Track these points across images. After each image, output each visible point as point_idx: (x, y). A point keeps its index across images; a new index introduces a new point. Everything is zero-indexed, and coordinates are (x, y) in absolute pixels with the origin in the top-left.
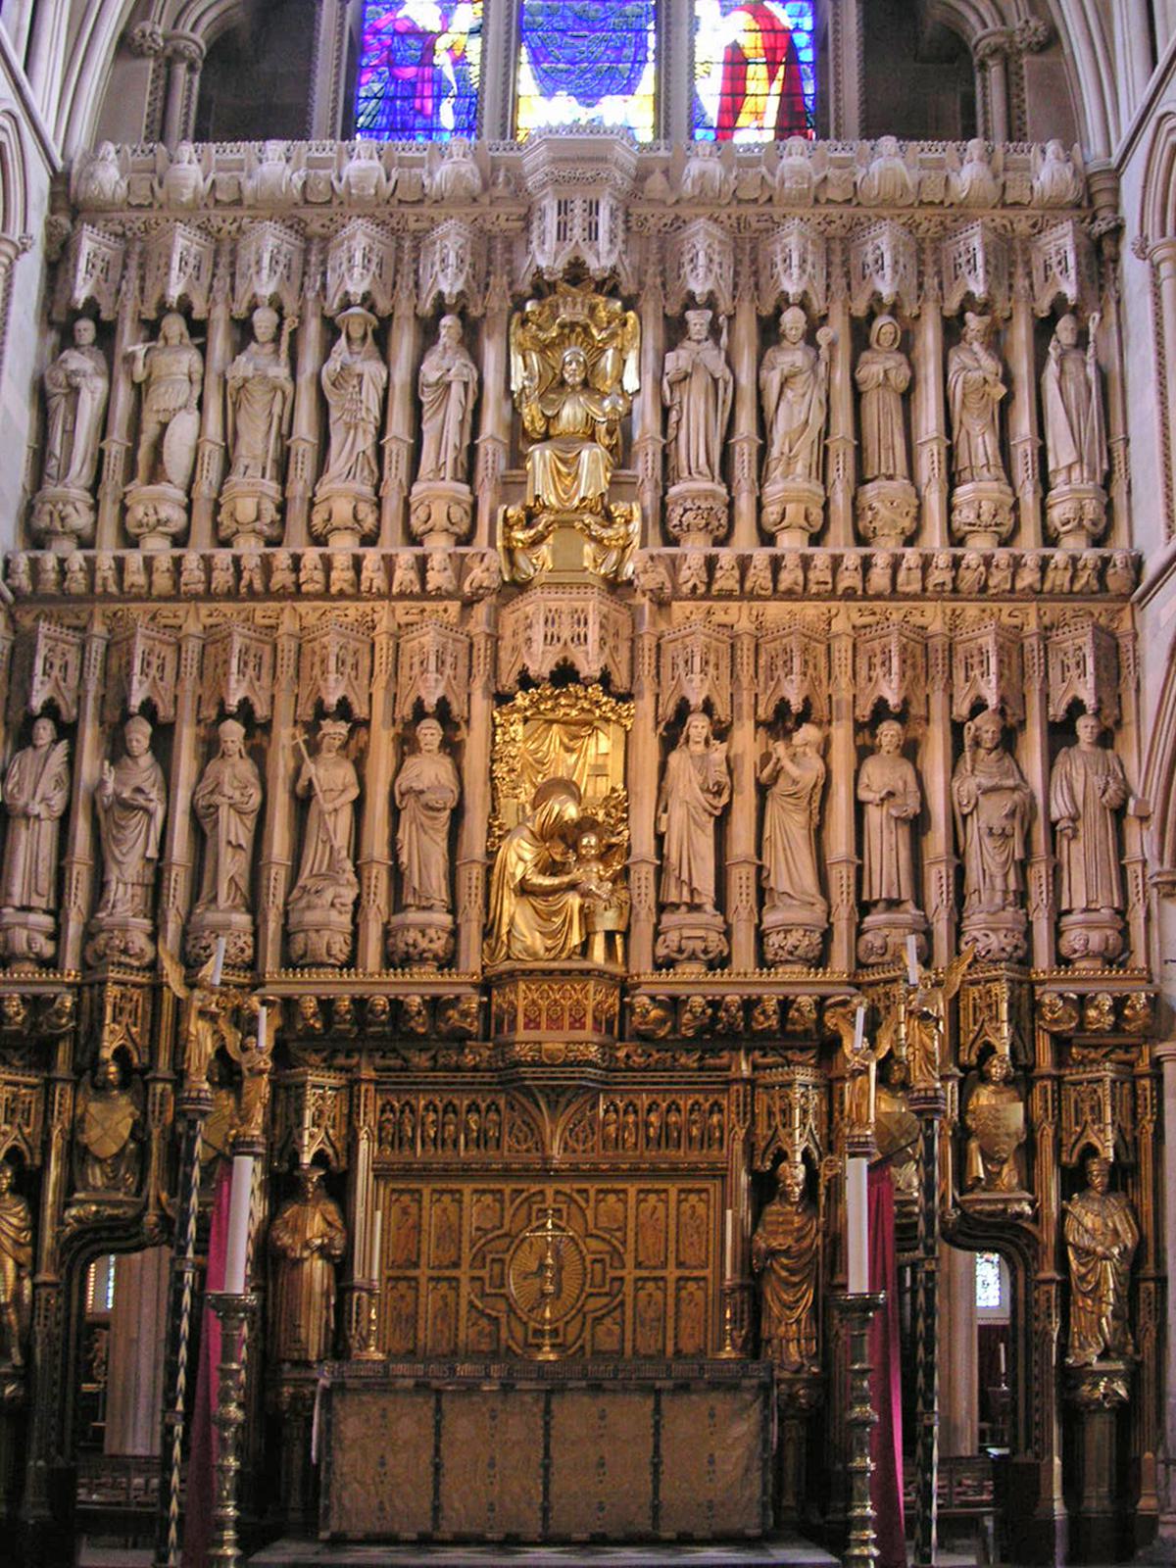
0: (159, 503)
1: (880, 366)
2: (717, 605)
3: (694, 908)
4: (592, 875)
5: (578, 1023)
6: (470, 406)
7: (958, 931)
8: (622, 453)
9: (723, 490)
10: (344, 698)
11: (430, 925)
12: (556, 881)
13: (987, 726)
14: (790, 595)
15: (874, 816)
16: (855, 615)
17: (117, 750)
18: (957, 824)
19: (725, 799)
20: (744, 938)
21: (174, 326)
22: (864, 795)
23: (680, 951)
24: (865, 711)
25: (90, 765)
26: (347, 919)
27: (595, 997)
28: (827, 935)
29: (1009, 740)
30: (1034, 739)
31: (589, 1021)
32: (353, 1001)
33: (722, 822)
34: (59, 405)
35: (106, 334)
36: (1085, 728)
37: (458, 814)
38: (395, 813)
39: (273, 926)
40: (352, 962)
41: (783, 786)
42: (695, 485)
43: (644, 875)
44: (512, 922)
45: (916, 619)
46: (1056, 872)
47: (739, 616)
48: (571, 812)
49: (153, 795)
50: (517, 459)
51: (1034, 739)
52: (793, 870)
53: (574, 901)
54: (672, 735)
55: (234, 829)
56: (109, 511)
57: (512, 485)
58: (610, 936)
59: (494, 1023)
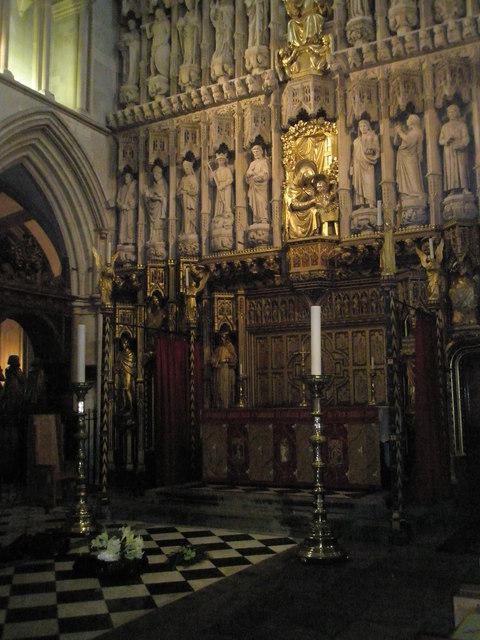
0: (155, 82)
2: (370, 71)
3: (367, 206)
5: (315, 262)
6: (266, 12)
9: (369, 18)
10: (224, 144)
11: (258, 229)
12: (306, 204)
14: (398, 58)
15: (447, 151)
16: (431, 59)
17: (152, 182)
19: (376, 157)
22: (442, 142)
23: (359, 226)
24: (440, 104)
25: (143, 187)
26: (230, 231)
28: (427, 209)
31: (319, 260)
32: (228, 264)
33: (377, 166)
34: (124, 54)
37: (270, 181)
38: (247, 187)
39: (204, 238)
40: (234, 248)
41: (403, 145)
43: (344, 196)
44: (289, 224)
45: (463, 54)
47: (377, 73)
48: (311, 173)
49: (160, 194)
53: (314, 211)
54: (353, 131)
58: (331, 224)
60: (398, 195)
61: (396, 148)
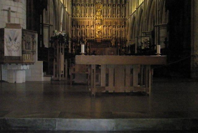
0: (78, 15)
1: (114, 7)
4: (100, 34)
7: (117, 36)
8: (101, 12)
13: (119, 26)
17: (77, 27)
18: (118, 31)
20: (107, 37)
21: (78, 5)
25: (76, 28)
27: (101, 39)
29: (120, 27)
30: (121, 27)
34: (73, 9)
35: (75, 5)
36: (124, 26)
37: (94, 30)
40: (89, 38)
42: (105, 14)
46: (122, 34)
50: (96, 12)
51: (121, 27)
52: (110, 33)
54: (104, 27)
55: (83, 31)
56: (76, 15)
57: (96, 14)
59: (96, 40)
60: (108, 34)
61: (108, 29)
